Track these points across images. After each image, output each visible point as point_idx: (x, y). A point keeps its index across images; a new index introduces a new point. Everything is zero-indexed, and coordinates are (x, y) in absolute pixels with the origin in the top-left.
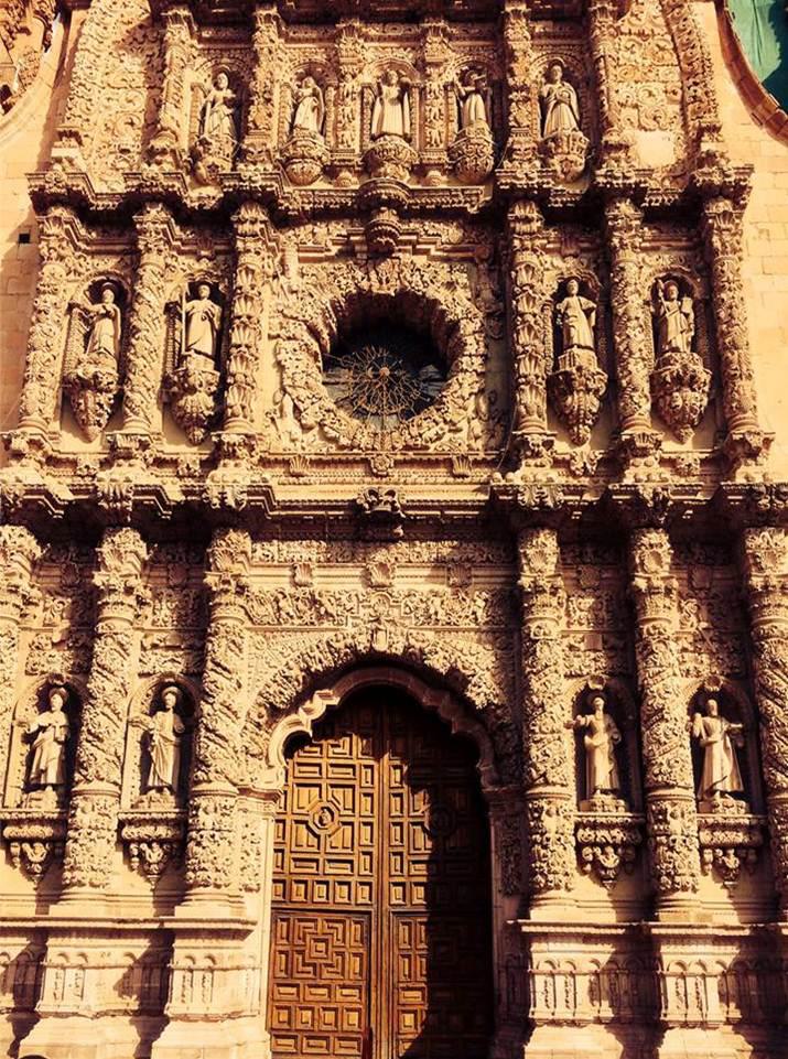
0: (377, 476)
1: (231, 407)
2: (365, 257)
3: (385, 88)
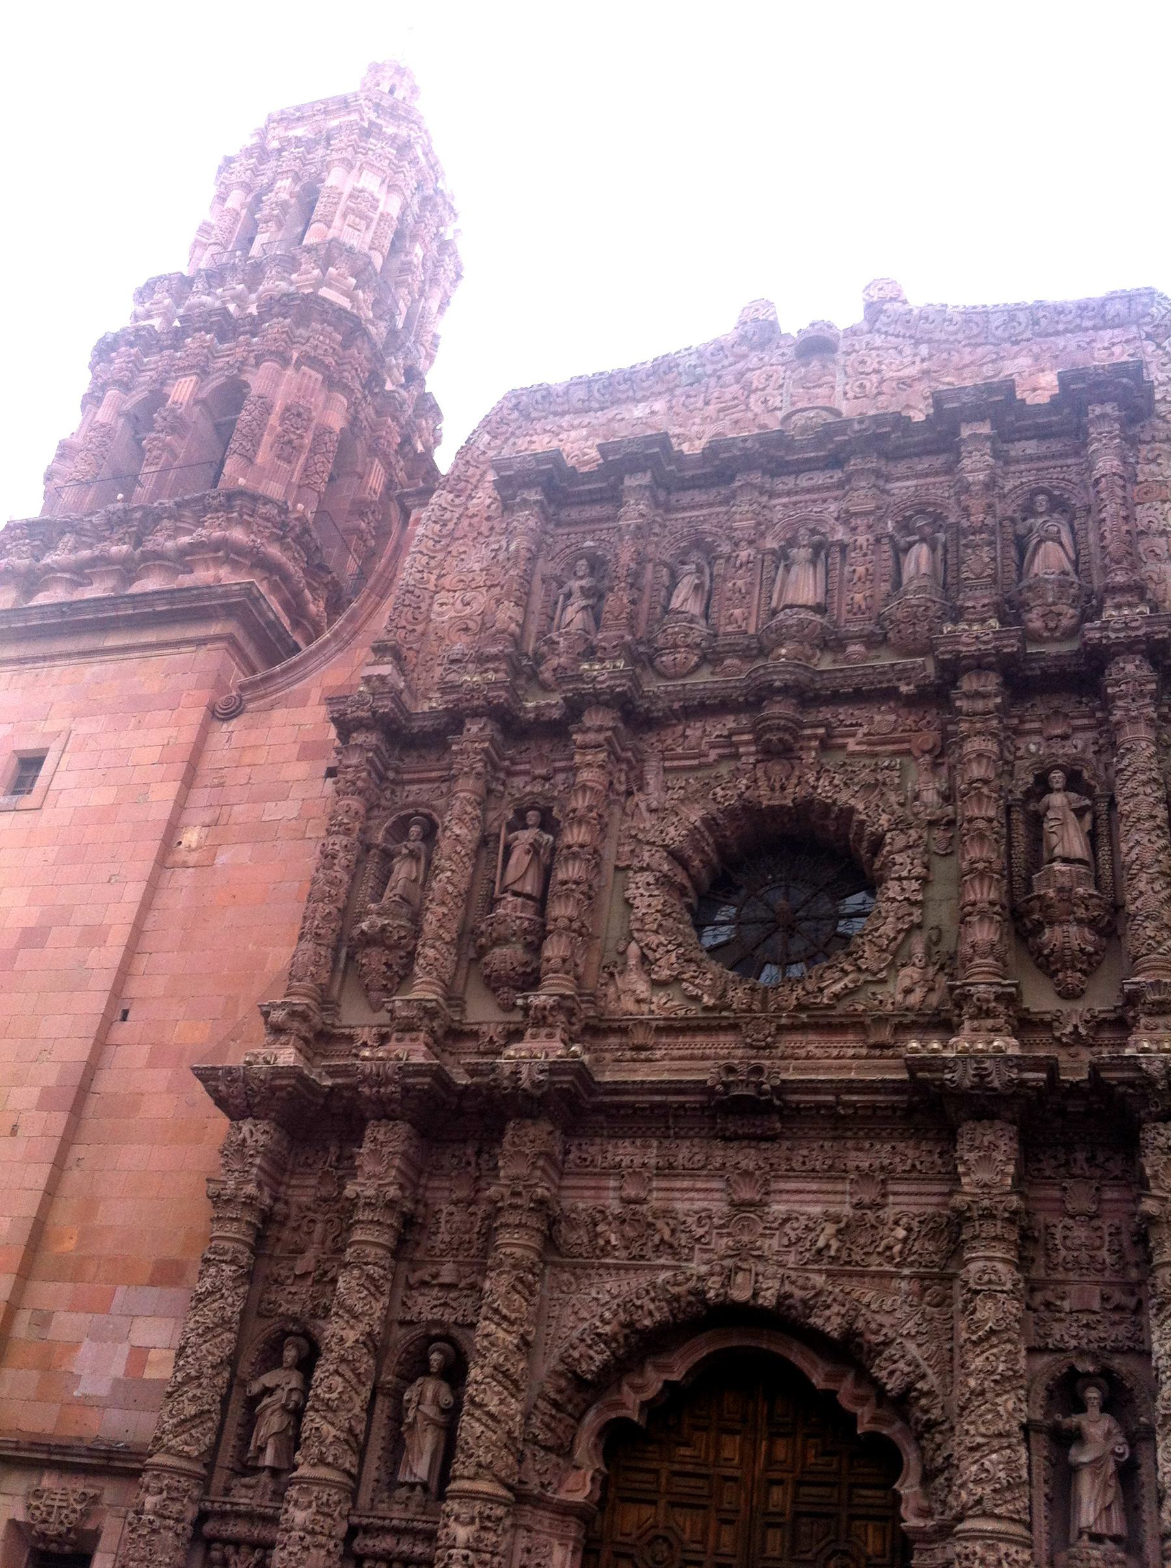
0: (752, 1047)
1: (548, 960)
2: (752, 760)
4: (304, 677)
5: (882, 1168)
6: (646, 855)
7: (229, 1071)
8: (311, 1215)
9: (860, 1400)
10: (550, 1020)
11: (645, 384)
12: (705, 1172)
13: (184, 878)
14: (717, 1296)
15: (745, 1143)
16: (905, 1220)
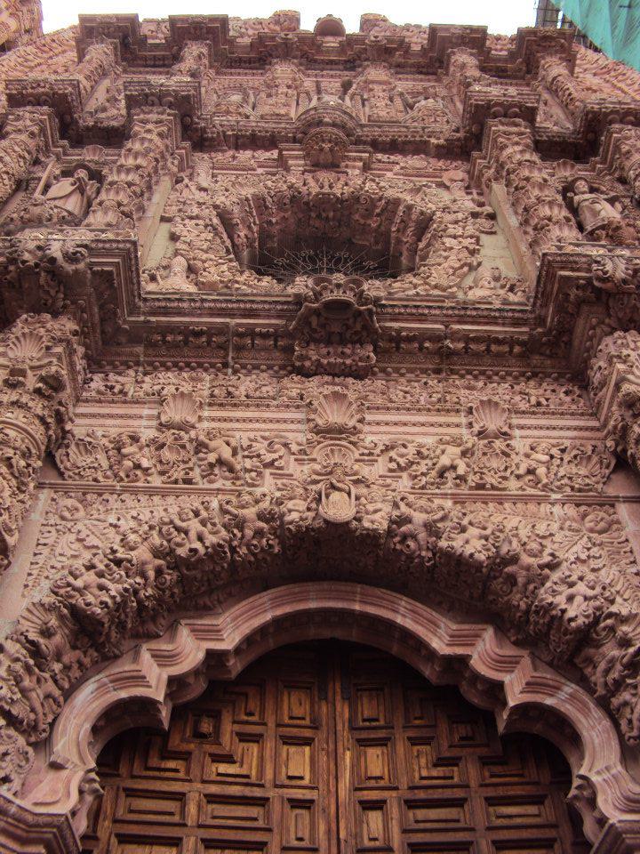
9: (508, 664)
14: (301, 519)
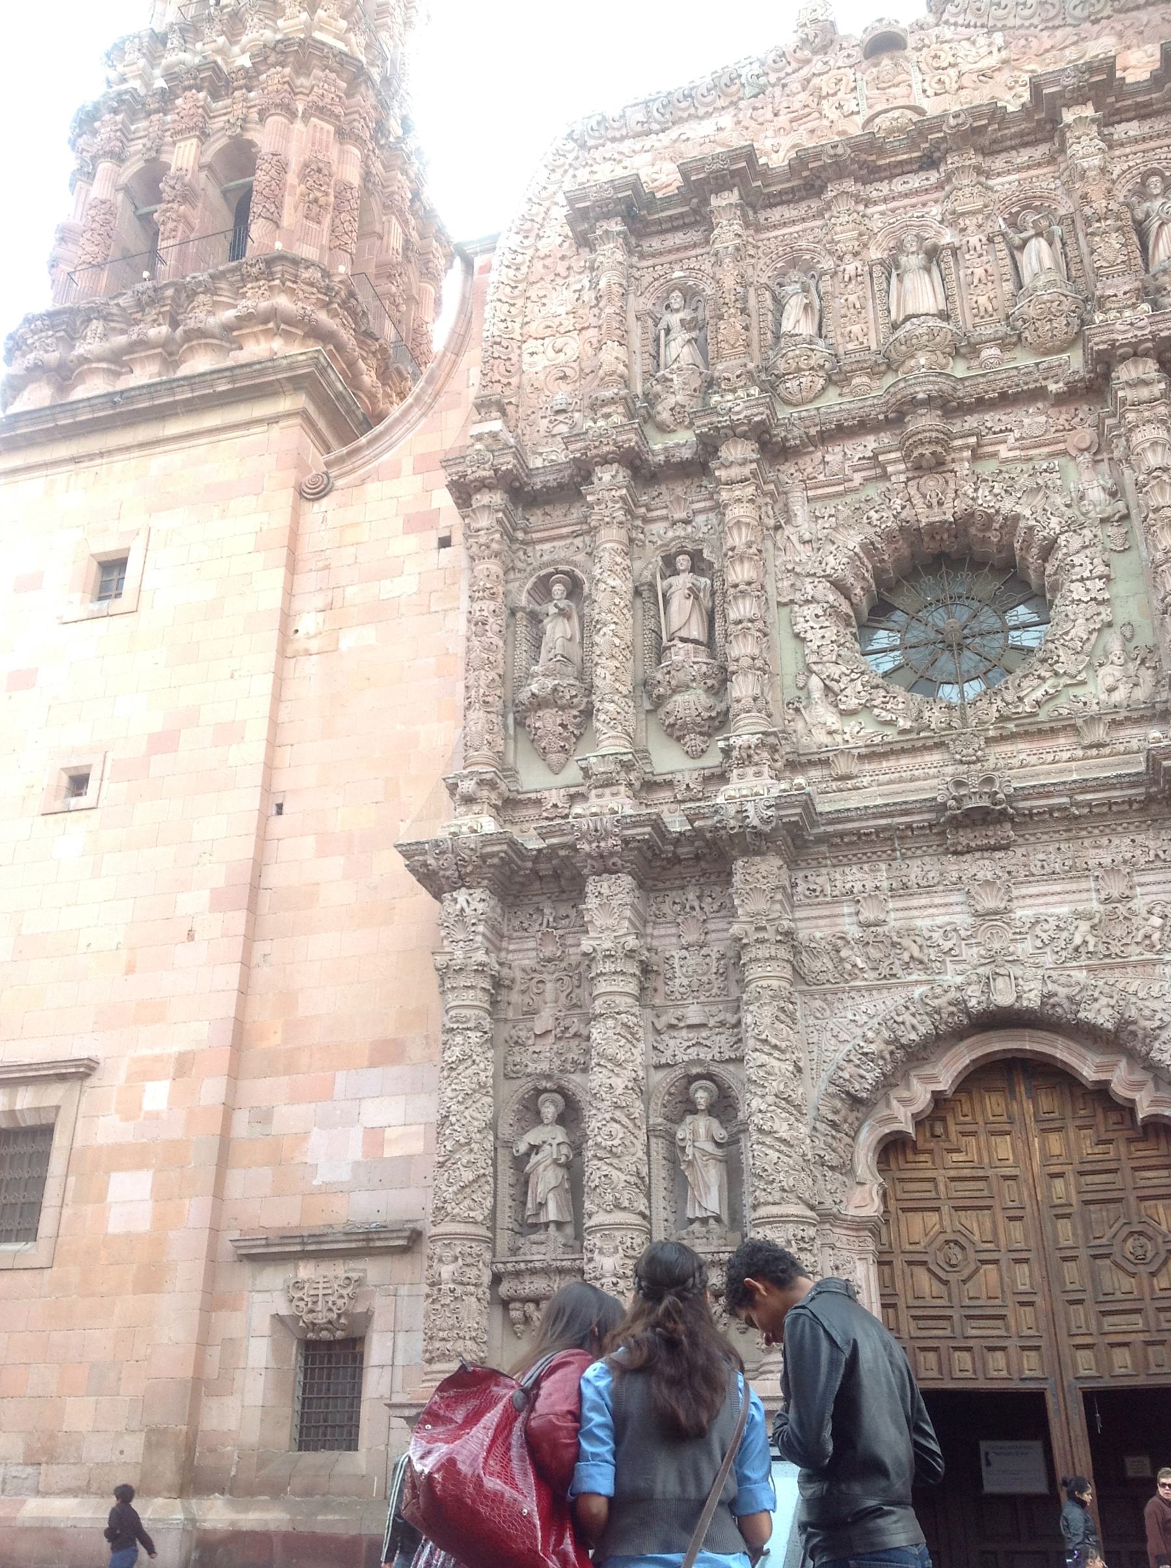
0: (961, 762)
1: (738, 701)
2: (903, 478)
3: (903, 259)
4: (390, 447)
5: (1125, 862)
6: (809, 587)
7: (436, 844)
8: (538, 977)
10: (756, 758)
11: (708, 99)
12: (941, 888)
13: (310, 666)
15: (978, 855)
16: (1159, 908)
